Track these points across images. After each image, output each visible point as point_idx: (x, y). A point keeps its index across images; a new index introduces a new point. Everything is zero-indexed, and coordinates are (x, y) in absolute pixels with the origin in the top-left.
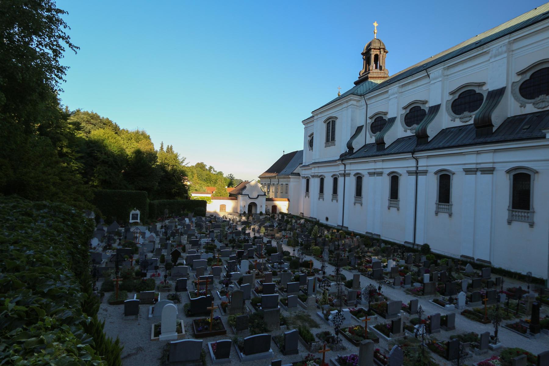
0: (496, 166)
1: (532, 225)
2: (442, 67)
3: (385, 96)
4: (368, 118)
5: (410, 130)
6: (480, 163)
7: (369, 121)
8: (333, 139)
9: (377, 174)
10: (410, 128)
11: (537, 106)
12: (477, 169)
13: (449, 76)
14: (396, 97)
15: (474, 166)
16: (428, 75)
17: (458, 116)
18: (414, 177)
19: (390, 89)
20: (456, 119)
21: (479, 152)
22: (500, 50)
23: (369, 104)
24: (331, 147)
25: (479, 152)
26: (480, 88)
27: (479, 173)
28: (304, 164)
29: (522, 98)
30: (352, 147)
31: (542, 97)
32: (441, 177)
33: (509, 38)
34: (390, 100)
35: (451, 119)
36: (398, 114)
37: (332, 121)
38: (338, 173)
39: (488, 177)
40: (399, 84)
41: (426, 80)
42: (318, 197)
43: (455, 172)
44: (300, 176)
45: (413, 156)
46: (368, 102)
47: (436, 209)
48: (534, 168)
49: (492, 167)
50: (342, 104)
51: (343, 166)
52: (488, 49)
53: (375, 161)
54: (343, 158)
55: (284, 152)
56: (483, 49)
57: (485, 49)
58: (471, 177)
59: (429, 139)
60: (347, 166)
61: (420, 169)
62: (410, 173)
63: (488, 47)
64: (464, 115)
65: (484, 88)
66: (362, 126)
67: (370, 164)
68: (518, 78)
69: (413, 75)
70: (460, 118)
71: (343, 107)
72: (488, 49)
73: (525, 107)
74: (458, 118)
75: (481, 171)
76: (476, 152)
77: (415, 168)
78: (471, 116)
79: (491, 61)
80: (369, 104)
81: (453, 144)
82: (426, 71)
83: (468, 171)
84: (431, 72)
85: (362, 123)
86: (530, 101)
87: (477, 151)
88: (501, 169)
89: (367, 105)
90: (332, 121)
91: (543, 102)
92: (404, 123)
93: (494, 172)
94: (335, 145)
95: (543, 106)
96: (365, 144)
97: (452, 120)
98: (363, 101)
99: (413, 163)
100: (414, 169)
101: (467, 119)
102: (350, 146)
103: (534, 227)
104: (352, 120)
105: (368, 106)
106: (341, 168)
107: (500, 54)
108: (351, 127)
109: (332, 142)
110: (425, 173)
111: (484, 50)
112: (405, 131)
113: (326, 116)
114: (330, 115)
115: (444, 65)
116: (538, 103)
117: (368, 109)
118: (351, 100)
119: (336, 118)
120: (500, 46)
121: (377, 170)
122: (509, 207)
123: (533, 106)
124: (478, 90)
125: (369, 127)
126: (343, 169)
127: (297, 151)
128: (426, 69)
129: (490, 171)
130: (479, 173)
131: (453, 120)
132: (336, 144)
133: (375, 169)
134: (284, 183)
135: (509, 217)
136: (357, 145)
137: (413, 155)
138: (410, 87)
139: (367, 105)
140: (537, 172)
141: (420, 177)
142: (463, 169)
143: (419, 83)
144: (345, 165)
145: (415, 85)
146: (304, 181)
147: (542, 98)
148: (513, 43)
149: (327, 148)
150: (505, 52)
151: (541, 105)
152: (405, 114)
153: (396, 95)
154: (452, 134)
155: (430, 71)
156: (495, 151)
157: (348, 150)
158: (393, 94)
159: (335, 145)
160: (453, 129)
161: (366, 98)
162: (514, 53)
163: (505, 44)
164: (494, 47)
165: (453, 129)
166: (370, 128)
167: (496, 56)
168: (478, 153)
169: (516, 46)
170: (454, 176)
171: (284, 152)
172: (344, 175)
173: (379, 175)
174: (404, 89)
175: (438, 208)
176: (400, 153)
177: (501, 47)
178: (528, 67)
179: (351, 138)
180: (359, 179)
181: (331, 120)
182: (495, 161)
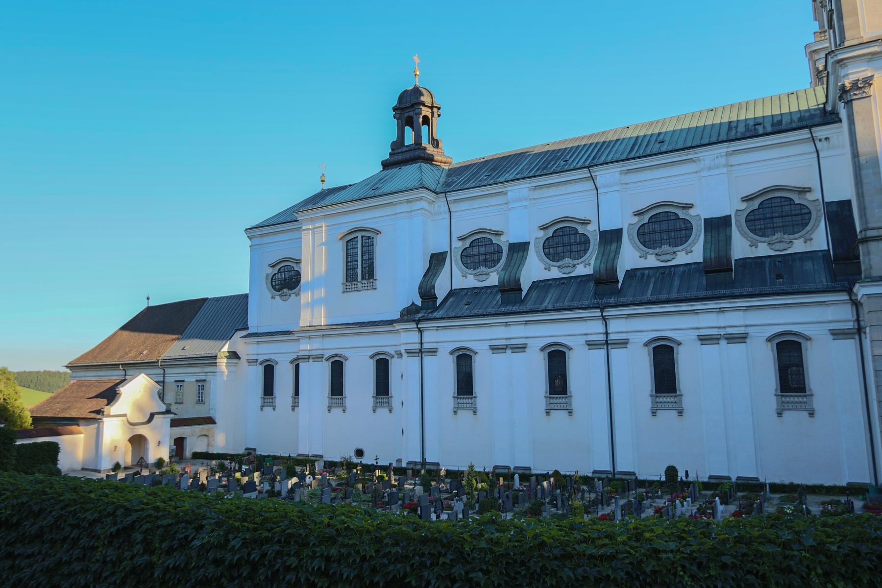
0: (749, 330)
1: (812, 414)
2: (619, 169)
3: (500, 200)
4: (454, 238)
5: (559, 267)
6: (725, 327)
8: (369, 273)
9: (512, 348)
10: (558, 264)
11: (773, 247)
13: (628, 186)
14: (526, 207)
15: (715, 332)
16: (592, 176)
17: (651, 251)
18: (602, 352)
19: (508, 189)
20: (649, 256)
21: (722, 310)
22: (717, 161)
23: (454, 212)
24: (362, 292)
25: (722, 310)
26: (684, 211)
28: (250, 331)
29: (751, 234)
30: (435, 295)
31: (778, 235)
32: (459, 358)
33: (728, 147)
35: (640, 254)
37: (362, 236)
40: (530, 183)
41: (589, 185)
42: (327, 405)
43: (681, 341)
45: (602, 314)
46: (453, 208)
47: (653, 405)
48: (807, 333)
49: (744, 332)
50: (395, 205)
52: (696, 156)
53: (506, 323)
54: (410, 314)
55: (148, 299)
56: (687, 155)
57: (692, 154)
58: (710, 349)
60: (425, 334)
61: (611, 337)
62: (592, 345)
63: (696, 153)
64: (661, 251)
65: (692, 212)
67: (493, 329)
68: (743, 206)
69: (561, 172)
70: (656, 255)
71: (398, 211)
72: (696, 156)
73: (756, 247)
74: (652, 254)
75: (727, 339)
76: (718, 310)
77: (602, 335)
78: (674, 253)
79: (703, 174)
82: (589, 170)
83: (704, 340)
86: (763, 239)
87: (720, 308)
89: (450, 212)
90: (362, 236)
91: (780, 242)
93: (748, 340)
95: (781, 249)
97: (640, 257)
98: (442, 204)
100: (602, 337)
101: (668, 257)
102: (427, 293)
103: (815, 416)
105: (452, 214)
106: (408, 337)
109: (363, 282)
110: (624, 343)
111: (689, 157)
112: (548, 269)
113: (352, 224)
114: (360, 223)
115: (622, 167)
116: (774, 243)
118: (421, 199)
119: (378, 232)
120: (716, 155)
121: (512, 340)
122: (776, 390)
123: (768, 247)
124: (681, 214)
126: (418, 340)
127: (204, 300)
128: (588, 167)
129: (521, 348)
130: (723, 342)
133: (506, 339)
135: (778, 405)
137: (602, 312)
138: (552, 191)
139: (450, 212)
140: (810, 339)
141: (427, 359)
142: (830, 330)
143: (570, 188)
145: (562, 189)
147: (779, 237)
148: (731, 155)
149: (349, 294)
150: (724, 166)
151: (778, 246)
152: (545, 239)
153: (525, 203)
154: (653, 280)
155: (594, 172)
156: (748, 308)
158: (520, 200)
159: (375, 289)
160: (647, 272)
161: (448, 199)
162: (733, 168)
163: (723, 154)
164: (708, 155)
167: (710, 169)
168: (720, 311)
169: (735, 159)
170: (680, 347)
171: (148, 299)
173: (593, 347)
175: (654, 403)
176: (571, 309)
177: (717, 157)
178: (758, 192)
179: (425, 276)
181: (359, 235)
182: (748, 323)
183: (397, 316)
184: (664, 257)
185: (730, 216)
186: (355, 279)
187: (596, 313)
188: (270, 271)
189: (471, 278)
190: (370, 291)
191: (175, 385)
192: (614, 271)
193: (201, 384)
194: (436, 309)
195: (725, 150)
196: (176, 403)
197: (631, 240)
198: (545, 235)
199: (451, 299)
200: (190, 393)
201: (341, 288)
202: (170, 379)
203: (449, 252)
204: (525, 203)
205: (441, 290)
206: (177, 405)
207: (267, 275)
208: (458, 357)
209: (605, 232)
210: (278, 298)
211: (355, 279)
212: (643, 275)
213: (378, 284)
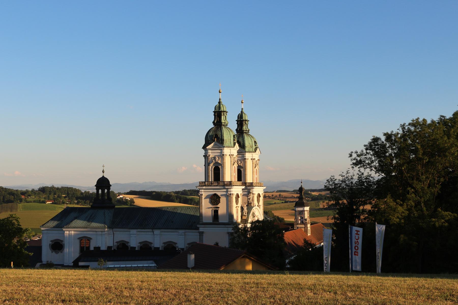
14: (135, 237)
19: (131, 230)
41: (152, 233)
46: (115, 233)
80: (115, 234)
84: (154, 231)
89: (114, 234)
105: (114, 235)
107: (182, 235)
111: (177, 231)
117: (114, 236)
153: (135, 236)
158: (134, 234)
167: (180, 235)
174: (138, 233)
188: (51, 243)
195: (184, 231)
204: (135, 236)
210: (54, 253)
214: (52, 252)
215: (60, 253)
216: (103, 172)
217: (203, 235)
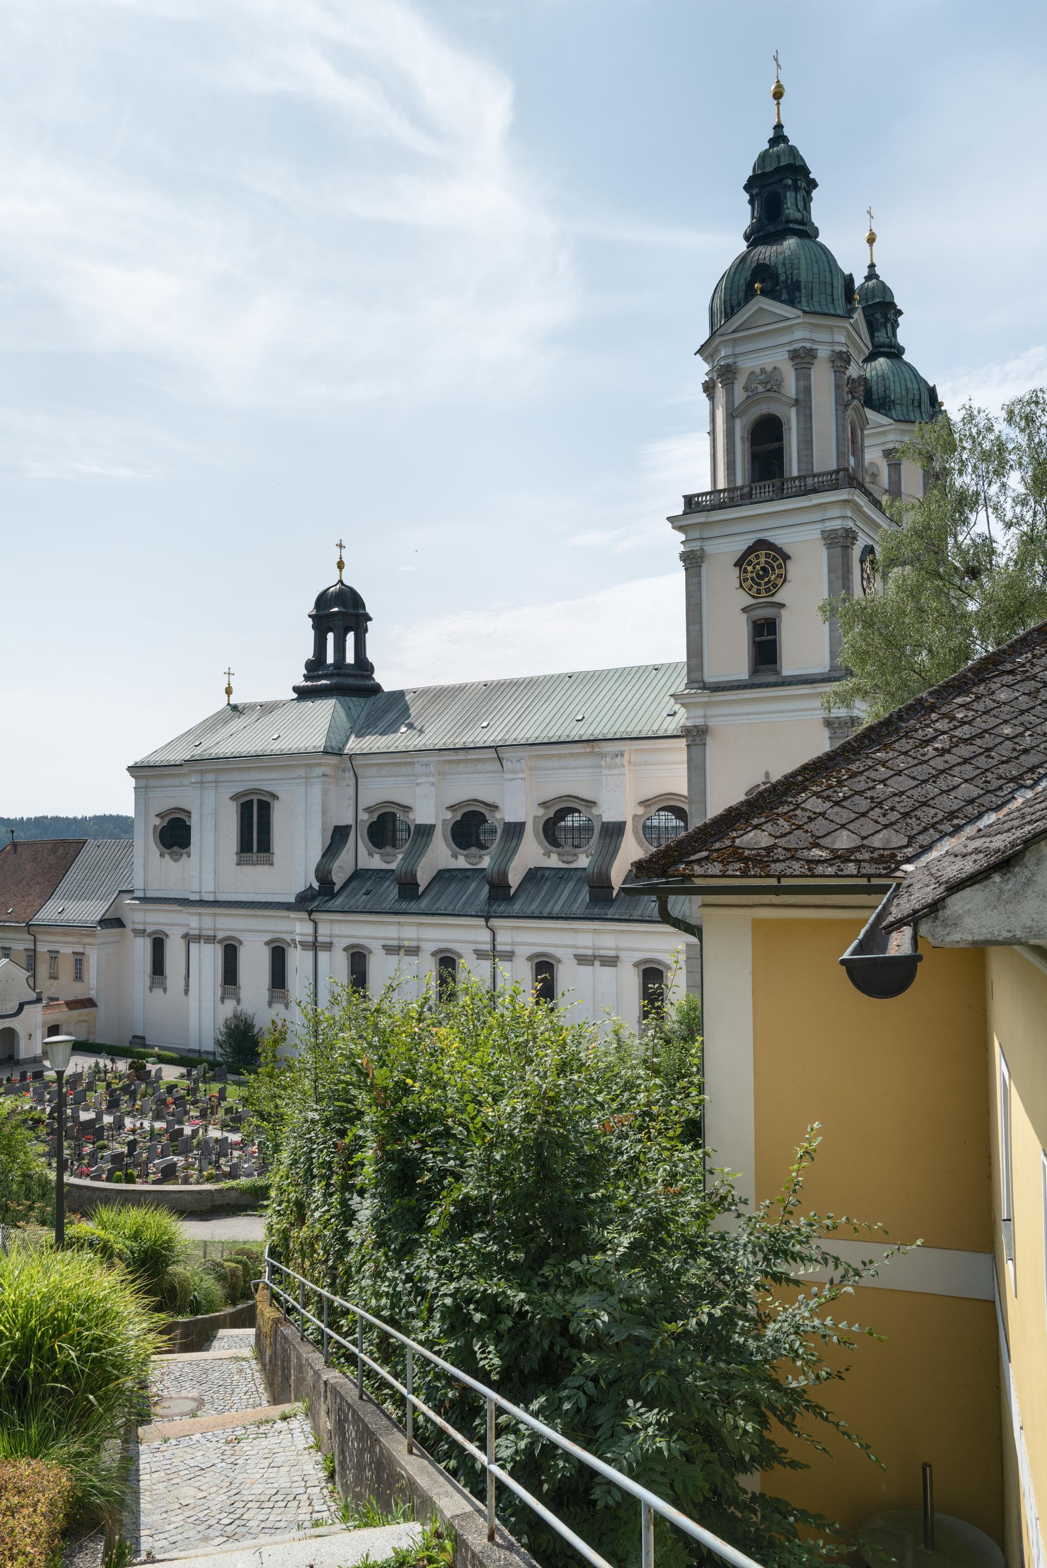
7: (363, 816)
8: (265, 846)
10: (465, 852)
12: (595, 957)
15: (589, 952)
17: (554, 849)
18: (487, 965)
19: (416, 760)
27: (597, 963)
34: (418, 784)
36: (436, 819)
38: (288, 938)
39: (608, 971)
44: (124, 926)
51: (311, 925)
58: (586, 970)
59: (512, 891)
62: (480, 955)
66: (349, 827)
70: (559, 854)
81: (557, 909)
85: (347, 818)
88: (628, 959)
90: (259, 800)
92: (450, 839)
94: (272, 864)
96: (356, 870)
99: (485, 936)
101: (569, 858)
104: (324, 812)
108: (324, 829)
110: (509, 956)
117: (360, 788)
125: (364, 830)
130: (597, 963)
131: (548, 854)
132: (275, 862)
134: (66, 950)
136: (341, 871)
137: (487, 921)
144: (315, 923)
146: (142, 948)
153: (432, 779)
157: (316, 885)
159: (272, 864)
160: (547, 873)
165: (547, 873)
166: (365, 832)
172: (315, 946)
179: (323, 856)
180: (358, 960)
183: (292, 899)
184: (566, 858)
185: (625, 823)
186: (250, 850)
187: (481, 922)
188: (157, 821)
189: (377, 857)
190: (266, 868)
191: (47, 957)
192: (505, 875)
193: (79, 957)
194: (334, 896)
196: (51, 978)
197: (536, 835)
198: (453, 817)
199: (354, 884)
200: (67, 969)
201: (234, 859)
202: (42, 948)
203: (353, 828)
204: (432, 779)
205: (339, 877)
206: (52, 981)
207: (155, 826)
208: (352, 955)
209: (509, 824)
210: (167, 856)
211: (250, 850)
212: (543, 876)
213: (276, 859)
214: (162, 855)
215: (185, 856)
216: (341, 565)
217: (705, 744)
